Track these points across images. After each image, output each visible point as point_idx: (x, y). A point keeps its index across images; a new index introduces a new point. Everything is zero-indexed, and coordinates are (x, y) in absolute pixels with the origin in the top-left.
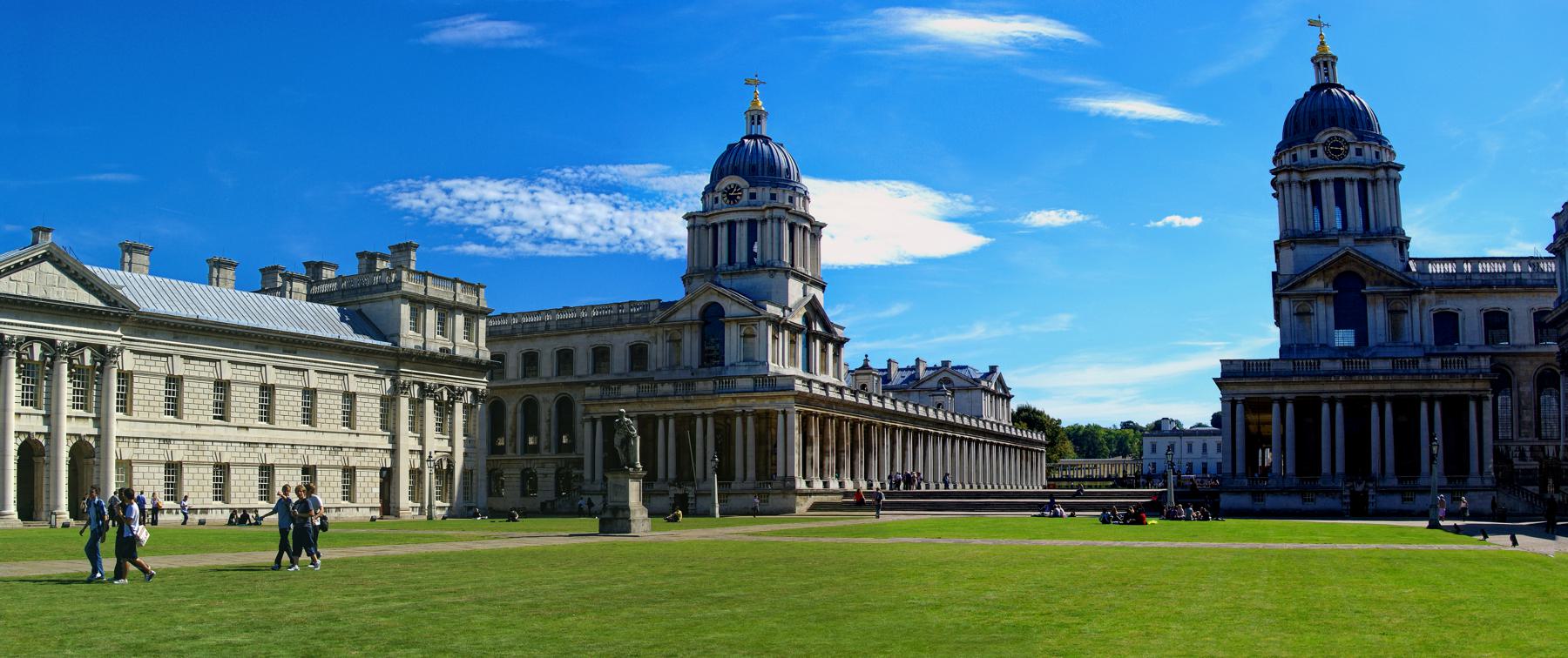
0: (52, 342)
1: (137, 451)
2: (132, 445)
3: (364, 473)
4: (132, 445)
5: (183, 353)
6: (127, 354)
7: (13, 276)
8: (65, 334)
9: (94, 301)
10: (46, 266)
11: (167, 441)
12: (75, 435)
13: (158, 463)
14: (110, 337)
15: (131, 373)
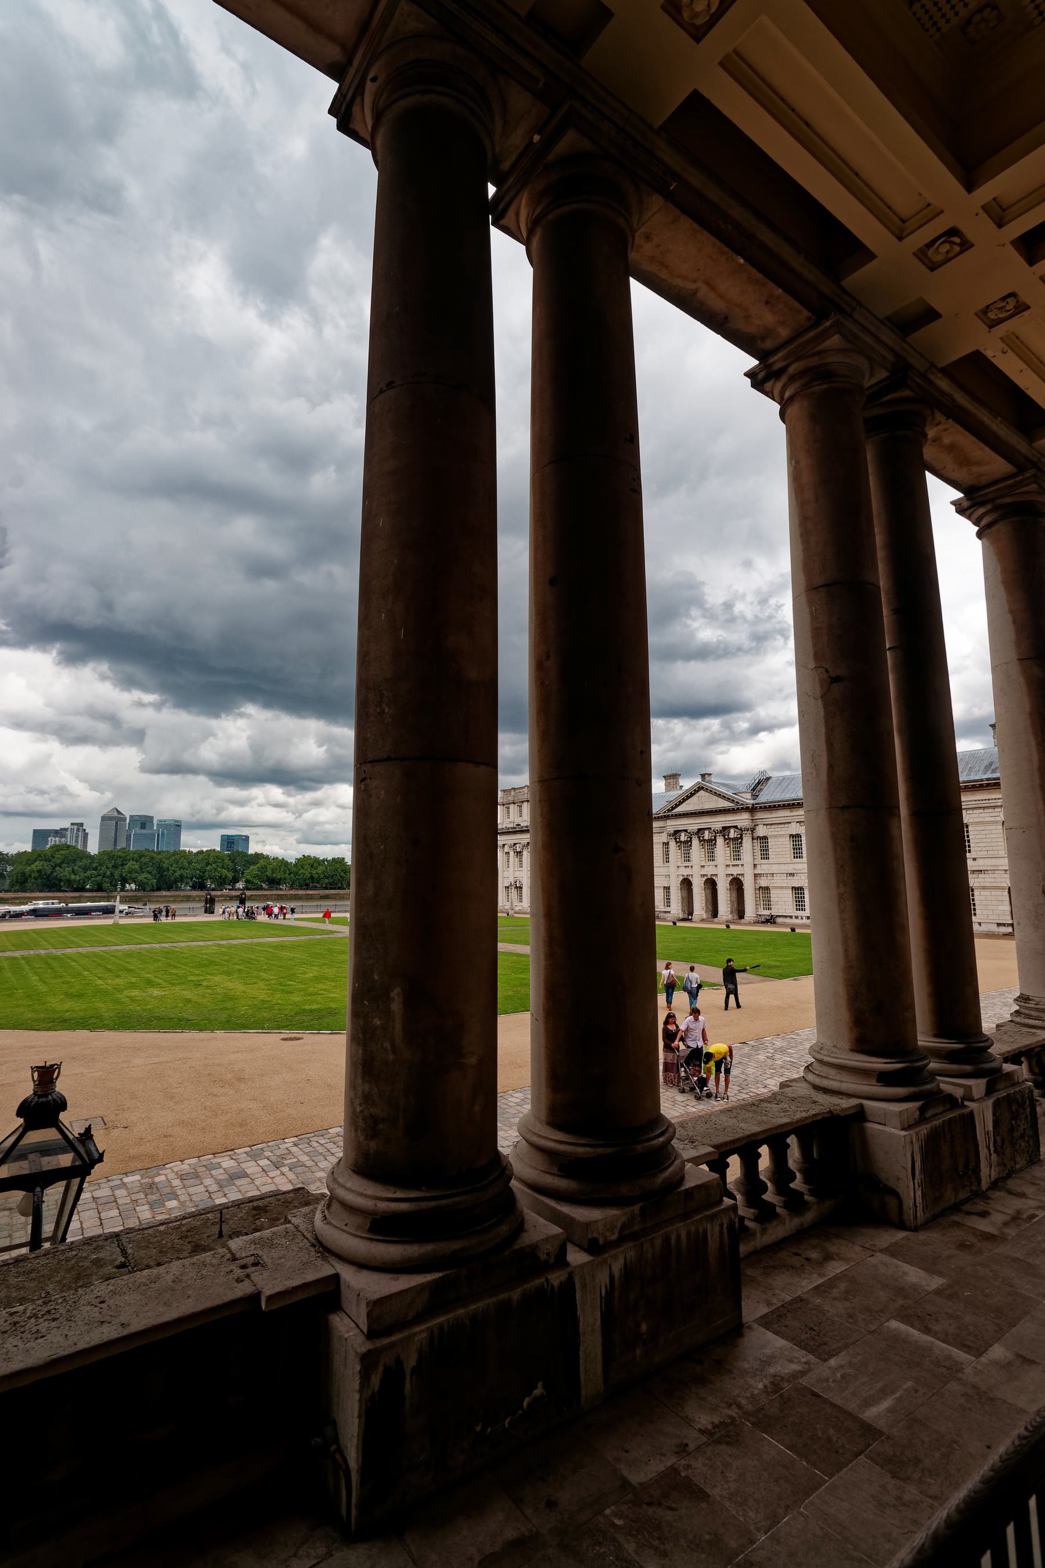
0: (710, 828)
1: (773, 881)
2: (769, 878)
3: (987, 893)
4: (769, 878)
5: (797, 820)
6: (761, 826)
7: (686, 802)
8: (718, 822)
9: (726, 804)
10: (702, 792)
11: (792, 875)
12: (732, 875)
13: (787, 888)
14: (743, 820)
15: (765, 838)
